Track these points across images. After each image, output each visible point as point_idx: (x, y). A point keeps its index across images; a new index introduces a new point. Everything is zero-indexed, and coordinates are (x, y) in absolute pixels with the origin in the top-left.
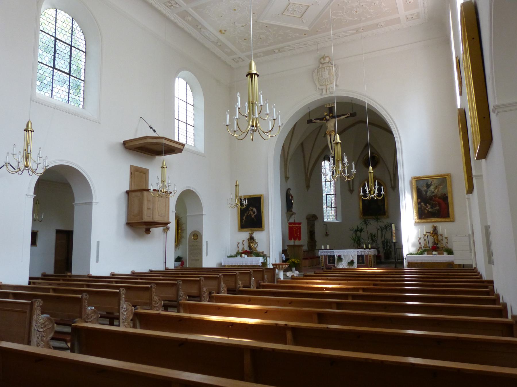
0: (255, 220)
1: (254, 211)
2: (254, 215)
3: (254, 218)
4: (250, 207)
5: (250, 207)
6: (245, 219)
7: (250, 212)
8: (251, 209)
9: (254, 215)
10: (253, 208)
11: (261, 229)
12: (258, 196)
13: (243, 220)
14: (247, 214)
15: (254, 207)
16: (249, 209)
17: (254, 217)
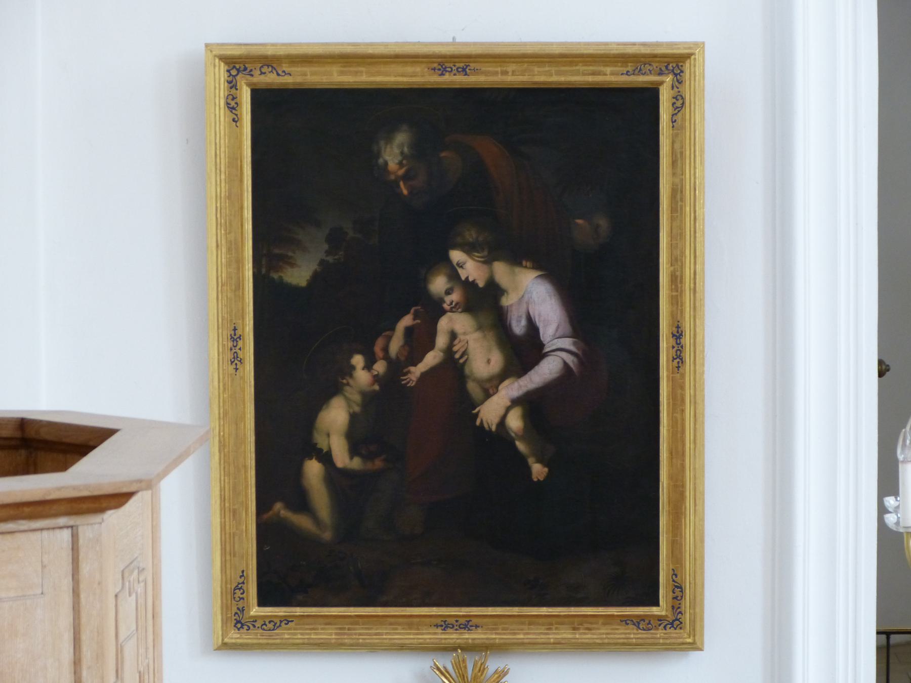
0: (538, 470)
1: (532, 328)
2: (512, 389)
3: (521, 446)
4: (456, 256)
5: (456, 256)
6: (354, 450)
7: (444, 324)
8: (469, 286)
9: (512, 389)
10: (501, 271)
11: (637, 622)
12: (611, 77)
13: (313, 469)
14: (397, 368)
15: (516, 259)
16: (439, 284)
17: (515, 422)
